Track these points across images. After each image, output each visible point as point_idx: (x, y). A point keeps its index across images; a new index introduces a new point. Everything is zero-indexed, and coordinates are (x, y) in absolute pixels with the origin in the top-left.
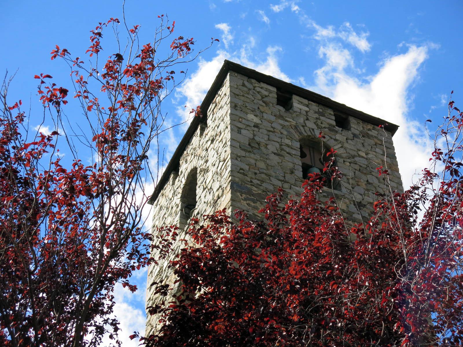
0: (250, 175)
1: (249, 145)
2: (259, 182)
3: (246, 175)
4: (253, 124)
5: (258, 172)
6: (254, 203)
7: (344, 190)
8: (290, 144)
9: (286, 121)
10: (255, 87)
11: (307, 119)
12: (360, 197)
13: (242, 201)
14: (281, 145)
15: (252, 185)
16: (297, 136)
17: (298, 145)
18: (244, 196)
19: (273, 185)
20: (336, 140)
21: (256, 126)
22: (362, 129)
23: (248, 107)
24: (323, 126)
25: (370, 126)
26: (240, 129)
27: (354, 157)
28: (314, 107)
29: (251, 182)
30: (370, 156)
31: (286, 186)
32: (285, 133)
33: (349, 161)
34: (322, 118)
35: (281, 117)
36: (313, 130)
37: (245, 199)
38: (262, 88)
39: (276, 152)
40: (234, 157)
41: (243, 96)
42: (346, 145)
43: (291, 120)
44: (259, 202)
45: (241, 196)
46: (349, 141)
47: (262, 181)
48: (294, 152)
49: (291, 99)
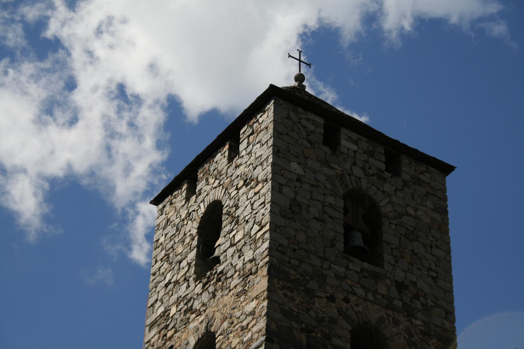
1: (290, 208)
2: (297, 263)
3: (285, 254)
4: (294, 178)
5: (296, 248)
6: (291, 292)
7: (386, 266)
8: (334, 203)
9: (332, 168)
10: (300, 119)
11: (354, 164)
12: (402, 274)
13: (279, 291)
14: (324, 206)
15: (289, 267)
16: (342, 191)
18: (281, 282)
19: (312, 265)
20: (384, 192)
21: (299, 180)
22: (413, 172)
23: (292, 152)
24: (371, 172)
25: (423, 168)
26: (281, 185)
28: (364, 144)
29: (290, 262)
30: (419, 213)
31: (326, 265)
32: (329, 186)
33: (395, 222)
34: (371, 160)
35: (326, 163)
36: (360, 178)
37: (282, 288)
38: (308, 120)
39: (317, 216)
41: (287, 134)
42: (395, 199)
43: (337, 167)
44: (296, 291)
45: (278, 283)
46: (398, 193)
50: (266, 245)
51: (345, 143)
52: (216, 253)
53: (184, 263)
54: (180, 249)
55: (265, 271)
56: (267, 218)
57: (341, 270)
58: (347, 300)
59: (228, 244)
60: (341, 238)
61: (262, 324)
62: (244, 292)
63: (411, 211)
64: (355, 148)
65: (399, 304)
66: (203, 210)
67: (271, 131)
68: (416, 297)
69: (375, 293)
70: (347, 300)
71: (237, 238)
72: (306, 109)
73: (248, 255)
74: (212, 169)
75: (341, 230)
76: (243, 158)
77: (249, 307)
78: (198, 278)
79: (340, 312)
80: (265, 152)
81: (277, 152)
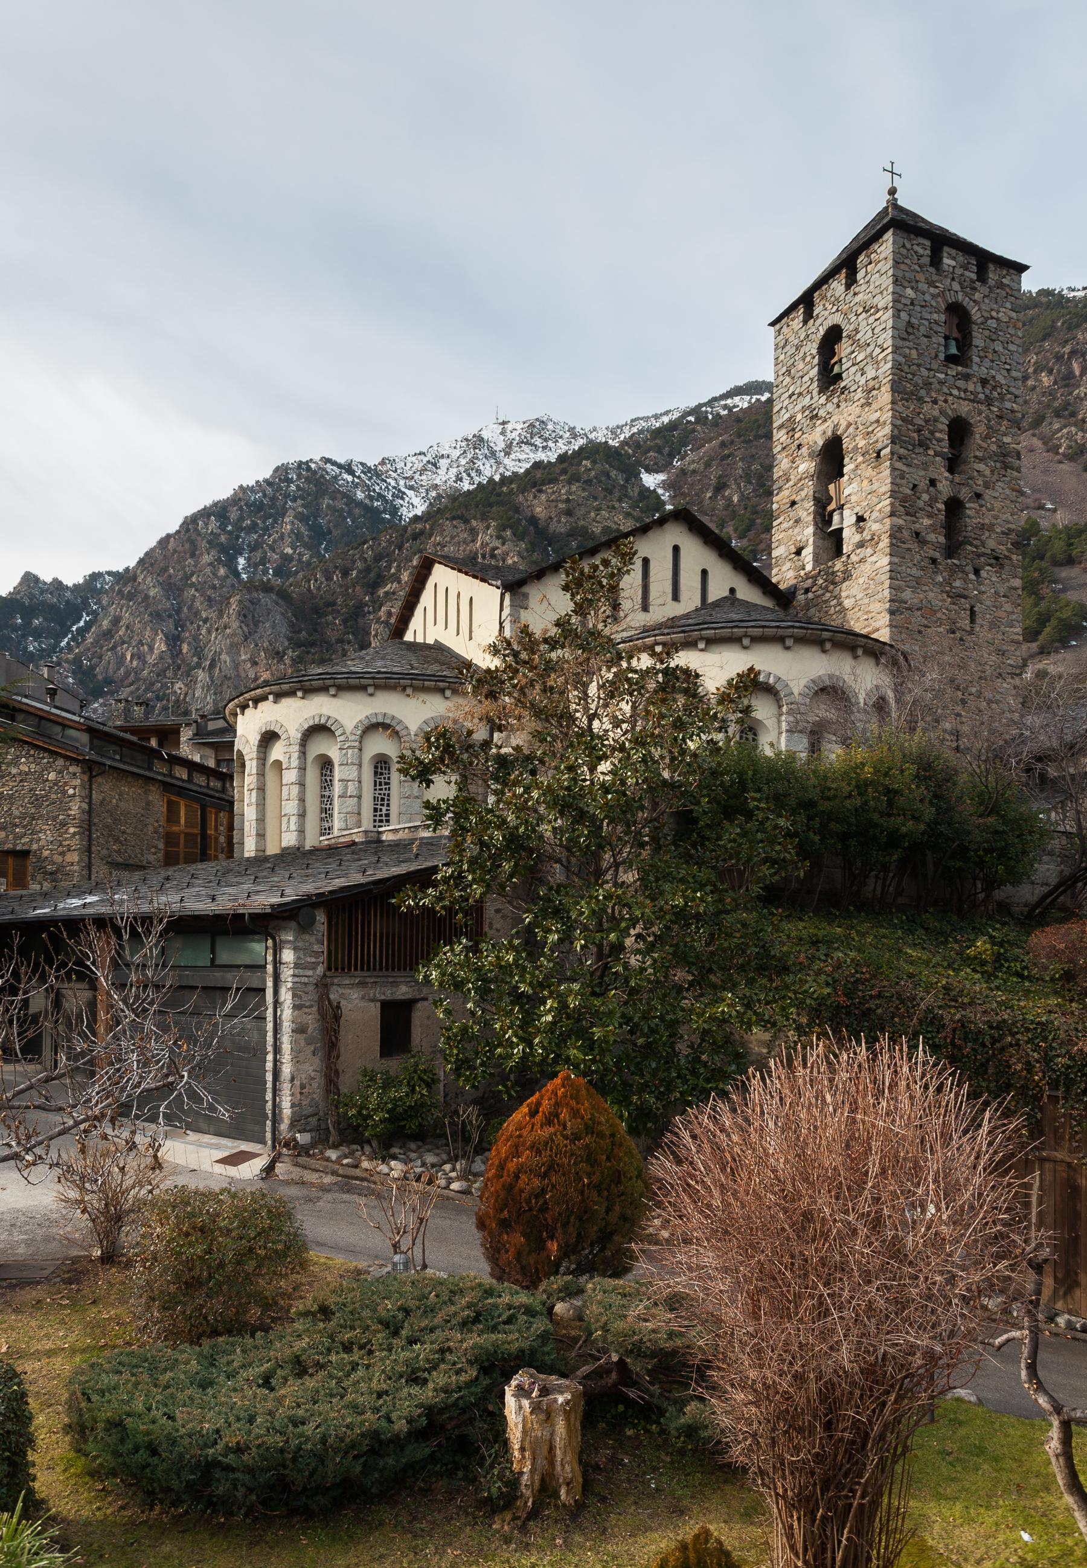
0: (906, 368)
7: (975, 367)
11: (953, 279)
17: (943, 318)
27: (987, 319)
34: (967, 273)
35: (932, 284)
40: (896, 350)
47: (914, 375)
48: (940, 329)
49: (940, 250)
50: (889, 365)
51: (947, 261)
52: (836, 370)
53: (806, 379)
54: (801, 366)
55: (888, 387)
56: (889, 342)
57: (942, 376)
58: (946, 401)
59: (850, 363)
60: (942, 348)
61: (887, 430)
62: (869, 404)
63: (994, 314)
64: (953, 263)
65: (982, 396)
66: (822, 332)
67: (890, 263)
68: (994, 388)
69: (966, 391)
70: (946, 401)
71: (859, 359)
72: (917, 235)
73: (871, 373)
74: (829, 295)
75: (942, 341)
76: (861, 287)
77: (874, 417)
78: (822, 390)
79: (942, 412)
80: (887, 282)
81: (896, 282)
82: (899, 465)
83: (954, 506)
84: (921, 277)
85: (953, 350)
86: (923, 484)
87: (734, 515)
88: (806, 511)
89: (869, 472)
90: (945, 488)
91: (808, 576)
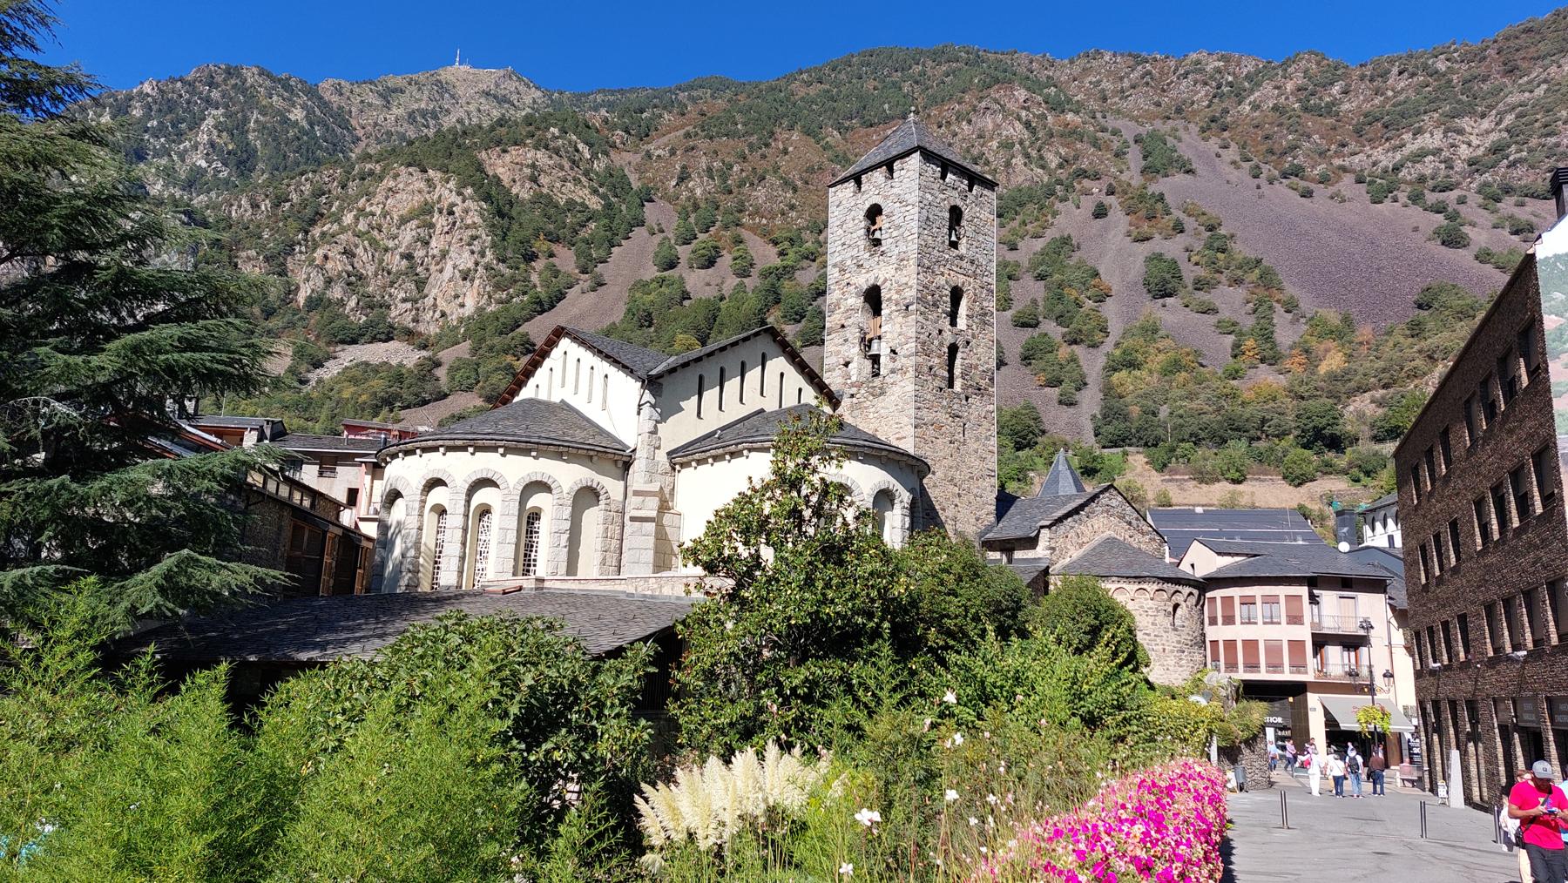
56: (915, 230)
66: (867, 206)
77: (904, 280)
82: (920, 318)
83: (953, 349)
84: (936, 186)
85: (954, 238)
86: (935, 333)
87: (696, 207)
88: (853, 334)
89: (900, 319)
90: (948, 338)
91: (853, 385)
